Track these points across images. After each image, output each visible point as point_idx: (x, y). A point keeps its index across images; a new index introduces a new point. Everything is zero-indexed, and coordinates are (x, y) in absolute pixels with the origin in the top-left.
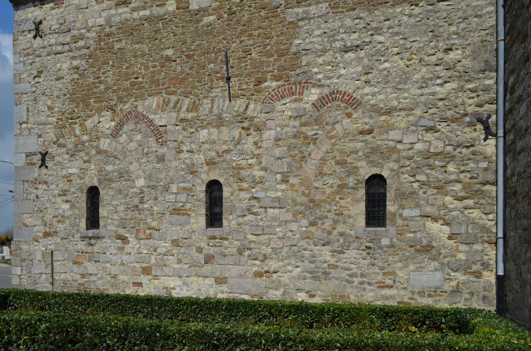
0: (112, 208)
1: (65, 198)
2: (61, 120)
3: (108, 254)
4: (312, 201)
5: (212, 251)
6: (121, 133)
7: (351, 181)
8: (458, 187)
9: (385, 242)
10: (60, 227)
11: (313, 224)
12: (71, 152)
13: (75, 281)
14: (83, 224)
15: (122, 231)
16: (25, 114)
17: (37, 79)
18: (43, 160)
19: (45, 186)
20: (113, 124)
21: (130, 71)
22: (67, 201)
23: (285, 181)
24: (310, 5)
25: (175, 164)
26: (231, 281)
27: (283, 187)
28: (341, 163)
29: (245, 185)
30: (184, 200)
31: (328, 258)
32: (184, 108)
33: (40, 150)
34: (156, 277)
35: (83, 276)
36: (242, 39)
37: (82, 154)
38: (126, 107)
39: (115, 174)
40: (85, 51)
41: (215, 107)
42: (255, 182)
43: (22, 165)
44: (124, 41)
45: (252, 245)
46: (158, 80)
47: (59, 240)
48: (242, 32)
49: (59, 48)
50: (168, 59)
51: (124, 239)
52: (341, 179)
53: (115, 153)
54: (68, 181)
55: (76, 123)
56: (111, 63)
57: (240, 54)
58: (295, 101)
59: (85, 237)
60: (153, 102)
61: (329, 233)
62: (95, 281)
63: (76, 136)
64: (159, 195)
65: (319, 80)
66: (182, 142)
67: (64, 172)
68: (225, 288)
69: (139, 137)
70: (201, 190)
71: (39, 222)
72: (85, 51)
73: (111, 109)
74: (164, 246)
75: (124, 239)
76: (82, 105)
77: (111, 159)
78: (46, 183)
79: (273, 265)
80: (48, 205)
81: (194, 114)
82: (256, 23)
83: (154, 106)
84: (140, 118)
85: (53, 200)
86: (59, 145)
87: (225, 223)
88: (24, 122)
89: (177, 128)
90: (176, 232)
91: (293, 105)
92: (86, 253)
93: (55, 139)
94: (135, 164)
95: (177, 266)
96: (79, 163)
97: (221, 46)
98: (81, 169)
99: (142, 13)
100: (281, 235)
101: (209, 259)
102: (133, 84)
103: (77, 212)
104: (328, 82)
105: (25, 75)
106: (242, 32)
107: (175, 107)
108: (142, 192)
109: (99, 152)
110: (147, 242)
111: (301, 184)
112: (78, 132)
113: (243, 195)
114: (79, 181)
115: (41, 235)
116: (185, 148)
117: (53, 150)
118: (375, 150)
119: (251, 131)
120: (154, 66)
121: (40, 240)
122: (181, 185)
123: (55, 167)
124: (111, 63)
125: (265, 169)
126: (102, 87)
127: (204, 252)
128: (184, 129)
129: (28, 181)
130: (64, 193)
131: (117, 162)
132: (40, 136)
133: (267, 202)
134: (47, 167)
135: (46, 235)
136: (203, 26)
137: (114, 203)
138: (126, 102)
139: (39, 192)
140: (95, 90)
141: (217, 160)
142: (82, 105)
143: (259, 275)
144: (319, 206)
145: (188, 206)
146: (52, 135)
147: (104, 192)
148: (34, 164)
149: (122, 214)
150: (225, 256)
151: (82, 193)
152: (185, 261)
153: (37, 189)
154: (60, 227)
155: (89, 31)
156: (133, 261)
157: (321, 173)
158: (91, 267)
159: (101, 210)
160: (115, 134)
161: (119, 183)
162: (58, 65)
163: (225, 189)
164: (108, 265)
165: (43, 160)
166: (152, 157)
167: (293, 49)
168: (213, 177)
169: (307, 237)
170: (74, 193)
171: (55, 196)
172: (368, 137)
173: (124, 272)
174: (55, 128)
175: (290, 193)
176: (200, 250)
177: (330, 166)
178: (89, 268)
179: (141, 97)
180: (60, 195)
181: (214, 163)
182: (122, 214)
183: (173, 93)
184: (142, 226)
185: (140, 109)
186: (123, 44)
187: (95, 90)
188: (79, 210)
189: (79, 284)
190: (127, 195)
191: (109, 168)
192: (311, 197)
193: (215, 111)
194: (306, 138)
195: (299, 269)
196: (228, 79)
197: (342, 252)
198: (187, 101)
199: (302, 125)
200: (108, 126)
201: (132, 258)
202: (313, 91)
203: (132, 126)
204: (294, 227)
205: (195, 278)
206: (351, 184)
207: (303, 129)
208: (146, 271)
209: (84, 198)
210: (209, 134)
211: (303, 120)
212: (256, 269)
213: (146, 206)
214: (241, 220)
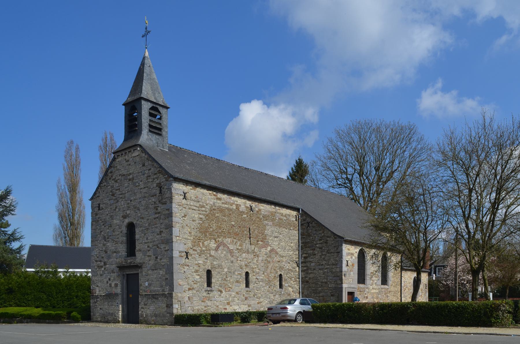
0: (216, 279)
1: (197, 273)
3: (215, 297)
4: (269, 280)
5: (247, 296)
6: (219, 249)
10: (195, 286)
12: (199, 254)
13: (203, 309)
14: (206, 285)
15: (220, 288)
16: (178, 232)
17: (183, 218)
18: (187, 256)
19: (188, 267)
22: (198, 275)
23: (263, 274)
25: (237, 264)
26: (252, 306)
27: (263, 275)
30: (239, 278)
31: (273, 298)
32: (238, 245)
33: (185, 251)
34: (231, 306)
35: (205, 307)
38: (220, 240)
39: (217, 266)
40: (204, 213)
41: (247, 246)
43: (177, 256)
44: (219, 214)
45: (257, 294)
50: (233, 225)
51: (221, 292)
54: (198, 266)
55: (201, 242)
57: (252, 231)
59: (207, 291)
60: (229, 240)
62: (210, 309)
63: (200, 247)
64: (232, 275)
66: (238, 257)
67: (196, 262)
68: (250, 308)
69: (225, 252)
71: (186, 284)
72: (204, 213)
74: (233, 294)
75: (221, 292)
76: (204, 235)
77: (215, 259)
78: (188, 266)
79: (262, 300)
80: (189, 276)
83: (229, 242)
84: (225, 245)
85: (192, 274)
86: (194, 250)
87: (250, 286)
89: (236, 251)
90: (237, 289)
91: (265, 251)
92: (207, 297)
93: (192, 247)
94: (224, 262)
95: (237, 301)
96: (203, 259)
98: (204, 262)
99: (225, 206)
100: (263, 290)
101: (246, 299)
103: (202, 280)
105: (178, 215)
107: (235, 244)
108: (227, 274)
109: (211, 256)
110: (228, 292)
111: (267, 275)
112: (201, 246)
114: (203, 267)
115: (187, 289)
116: (239, 259)
117: (191, 251)
118: (280, 267)
119: (256, 257)
120: (229, 227)
121: (186, 292)
123: (192, 259)
125: (259, 269)
126: (211, 229)
127: (245, 296)
129: (180, 264)
130: (196, 271)
131: (218, 261)
132: (185, 244)
134: (188, 259)
135: (189, 289)
137: (217, 277)
139: (185, 270)
140: (209, 230)
141: (248, 265)
142: (204, 235)
143: (258, 303)
146: (191, 245)
147: (214, 272)
149: (220, 282)
150: (250, 297)
151: (205, 272)
152: (240, 299)
153: (184, 268)
154: (195, 286)
155: (207, 205)
156: (224, 300)
157: (271, 272)
158: (209, 303)
159: (213, 280)
160: (217, 249)
161: (218, 269)
162: (193, 215)
164: (215, 302)
165: (187, 256)
166: (229, 261)
167: (265, 234)
168: (247, 271)
170: (201, 272)
171: (193, 272)
173: (221, 304)
174: (192, 242)
175: (264, 278)
177: (273, 271)
178: (208, 303)
179: (225, 237)
180: (195, 272)
181: (247, 266)
182: (220, 282)
184: (227, 286)
187: (209, 230)
188: (204, 279)
189: (204, 310)
190: (222, 274)
191: (215, 263)
193: (247, 248)
195: (267, 301)
196: (250, 238)
197: (275, 296)
200: (213, 246)
201: (223, 299)
202: (269, 247)
205: (242, 305)
207: (267, 258)
208: (228, 304)
209: (206, 274)
210: (246, 256)
211: (267, 255)
212: (257, 301)
213: (228, 279)
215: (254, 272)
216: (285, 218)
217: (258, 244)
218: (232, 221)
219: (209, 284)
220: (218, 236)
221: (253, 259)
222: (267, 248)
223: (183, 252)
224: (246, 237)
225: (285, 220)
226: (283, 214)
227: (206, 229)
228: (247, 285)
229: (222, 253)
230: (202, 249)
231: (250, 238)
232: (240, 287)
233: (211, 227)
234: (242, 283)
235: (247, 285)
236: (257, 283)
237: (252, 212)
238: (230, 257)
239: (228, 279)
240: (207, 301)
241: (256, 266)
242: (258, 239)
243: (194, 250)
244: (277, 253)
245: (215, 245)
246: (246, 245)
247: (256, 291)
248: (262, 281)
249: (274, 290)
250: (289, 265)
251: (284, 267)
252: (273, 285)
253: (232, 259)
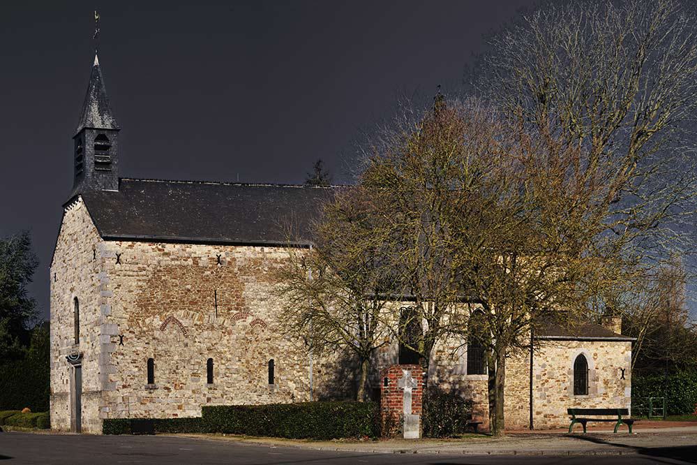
4: (250, 371)
5: (210, 396)
7: (263, 362)
8: (298, 367)
9: (275, 391)
11: (250, 382)
15: (168, 385)
17: (117, 290)
19: (122, 357)
20: (161, 323)
22: (136, 367)
25: (192, 348)
27: (239, 363)
28: (260, 353)
37: (144, 338)
40: (144, 278)
45: (227, 393)
47: (132, 390)
48: (223, 282)
49: (131, 273)
50: (189, 290)
58: (244, 321)
63: (140, 327)
67: (134, 349)
69: (175, 332)
71: (120, 379)
73: (160, 314)
78: (123, 354)
84: (175, 321)
86: (130, 332)
90: (194, 386)
93: (128, 328)
94: (173, 347)
95: (194, 404)
99: (176, 262)
102: (171, 301)
114: (143, 355)
116: (196, 340)
117: (127, 334)
125: (231, 354)
130: (134, 361)
132: (119, 325)
133: (232, 371)
135: (124, 387)
145: (199, 372)
160: (163, 328)
166: (181, 343)
167: (242, 296)
172: (269, 342)
176: (205, 395)
179: (176, 309)
185: (175, 316)
191: (160, 348)
196: (216, 306)
203: (172, 326)
204: (243, 383)
207: (247, 335)
208: (180, 407)
214: (222, 380)
217: (229, 314)
218: (186, 284)
219: (151, 378)
220: (165, 309)
222: (246, 318)
223: (116, 336)
227: (148, 301)
229: (172, 333)
232: (199, 383)
233: (154, 298)
234: (202, 376)
235: (210, 380)
236: (228, 377)
237: (221, 264)
238: (183, 338)
240: (148, 404)
241: (226, 349)
242: (229, 306)
244: (264, 325)
246: (210, 317)
247: (226, 389)
249: (258, 386)
250: (289, 343)
251: (279, 347)
253: (186, 341)
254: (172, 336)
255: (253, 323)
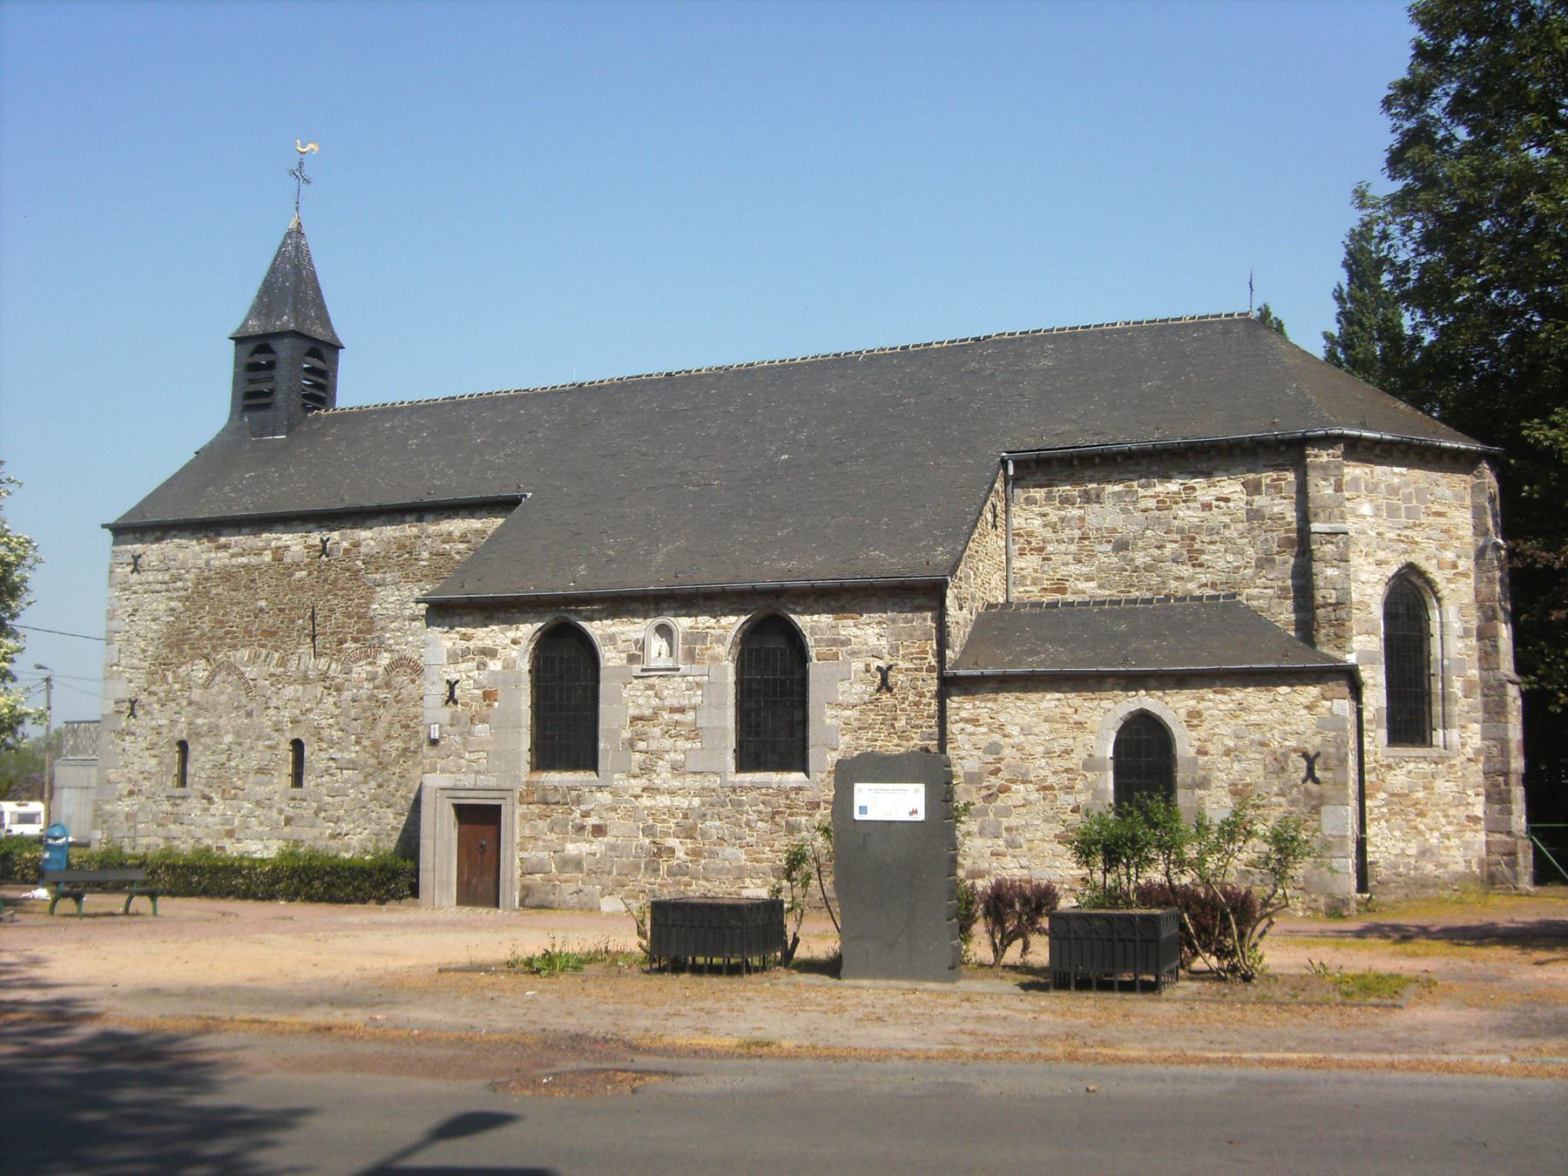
2: (154, 665)
11: (380, 786)
18: (132, 709)
21: (226, 618)
23: (358, 743)
24: (385, 573)
27: (357, 748)
28: (406, 727)
29: (325, 746)
36: (329, 597)
37: (173, 704)
42: (332, 744)
46: (251, 632)
48: (329, 591)
50: (261, 610)
52: (404, 742)
53: (205, 706)
56: (207, 608)
58: (370, 663)
60: (245, 653)
61: (393, 796)
65: (391, 645)
67: (154, 723)
70: (286, 747)
78: (133, 734)
81: (281, 669)
82: (341, 584)
84: (231, 668)
86: (150, 693)
87: (305, 783)
88: (115, 665)
91: (369, 668)
94: (224, 718)
97: (309, 603)
104: (398, 647)
106: (329, 591)
111: (373, 746)
112: (170, 679)
113: (323, 755)
117: (143, 697)
122: (266, 743)
124: (207, 608)
128: (272, 685)
130: (152, 746)
136: (295, 581)
138: (220, 652)
139: (127, 745)
141: (301, 718)
144: (385, 768)
148: (122, 713)
163: (306, 748)
165: (132, 709)
166: (242, 712)
168: (295, 736)
169: (374, 798)
175: (362, 755)
179: (234, 647)
181: (298, 722)
183: (264, 646)
186: (220, 590)
191: (200, 721)
192: (380, 760)
194: (377, 701)
198: (277, 655)
199: (374, 688)
202: (386, 655)
206: (412, 748)
207: (376, 691)
213: (233, 764)
215: (321, 740)
216: (462, 546)
218: (257, 600)
220: (214, 648)
221: (321, 699)
222: (375, 658)
223: (124, 701)
224: (299, 637)
225: (458, 553)
226: (450, 534)
228: (297, 780)
230: (171, 687)
231: (313, 639)
233: (196, 628)
234: (276, 774)
235: (297, 780)
236: (332, 775)
237: (327, 556)
238: (244, 701)
239: (233, 764)
241: (331, 721)
243: (150, 693)
245: (206, 673)
248: (351, 766)
252: (395, 778)
254: (223, 698)
255: (389, 669)
